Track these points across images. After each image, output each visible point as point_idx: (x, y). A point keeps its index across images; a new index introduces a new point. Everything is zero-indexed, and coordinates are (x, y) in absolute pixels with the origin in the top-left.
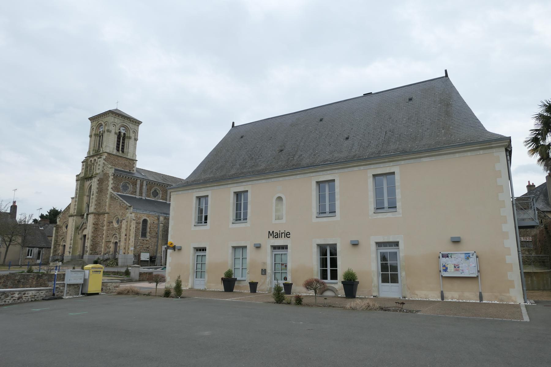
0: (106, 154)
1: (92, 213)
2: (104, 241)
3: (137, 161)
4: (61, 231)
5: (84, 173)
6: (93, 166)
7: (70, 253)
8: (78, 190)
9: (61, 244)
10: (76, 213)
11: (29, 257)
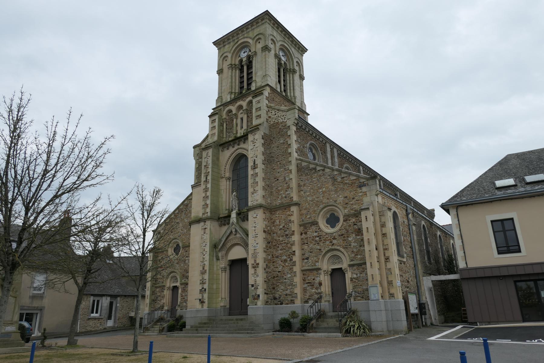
0: (268, 89)
1: (260, 206)
2: (297, 269)
3: (309, 115)
5: (217, 134)
6: (235, 120)
7: (202, 302)
8: (210, 166)
9: (168, 285)
10: (209, 214)
11: (94, 315)
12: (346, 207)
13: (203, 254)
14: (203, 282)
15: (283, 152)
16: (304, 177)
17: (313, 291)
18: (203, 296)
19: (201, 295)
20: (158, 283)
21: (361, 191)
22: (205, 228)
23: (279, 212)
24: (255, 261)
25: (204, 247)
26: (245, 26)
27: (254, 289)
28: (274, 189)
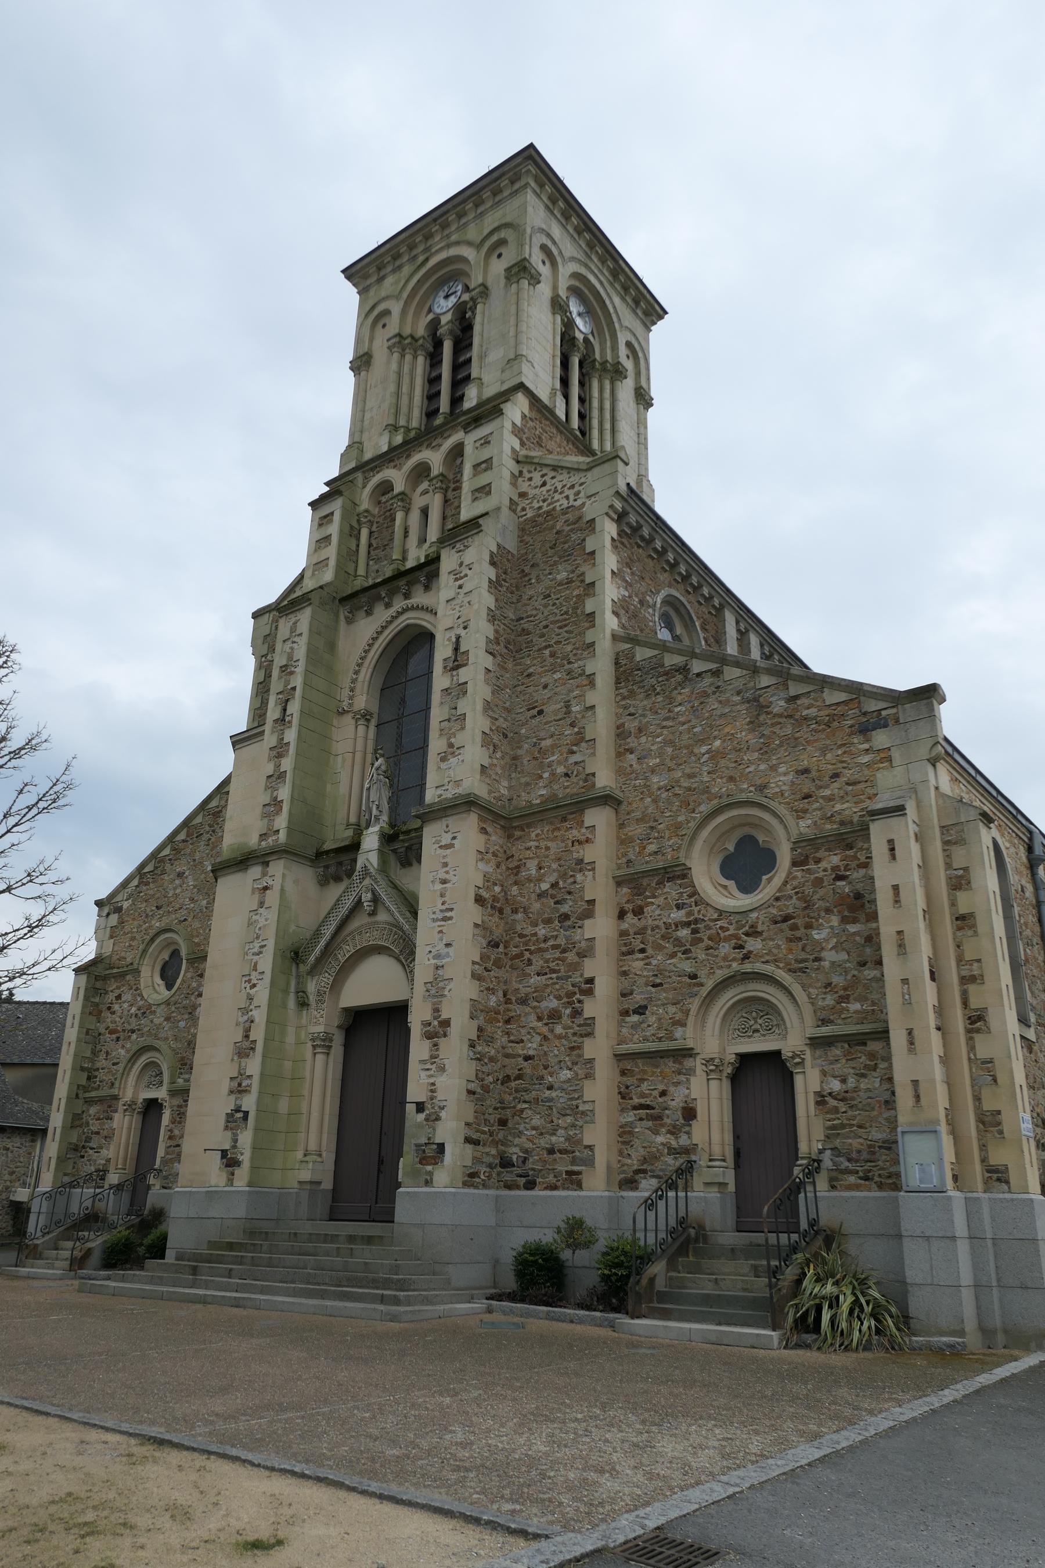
1: (468, 803)
4: (127, 997)
5: (332, 563)
6: (399, 516)
7: (230, 1161)
8: (300, 669)
9: (128, 1095)
10: (282, 836)
12: (805, 811)
13: (249, 981)
14: (240, 1085)
15: (566, 613)
16: (640, 703)
17: (660, 1139)
18: (236, 1141)
19: (229, 1134)
20: (97, 1089)
21: (866, 746)
22: (266, 888)
23: (539, 831)
24: (436, 1010)
25: (256, 958)
26: (455, 207)
27: (427, 1120)
28: (526, 746)
